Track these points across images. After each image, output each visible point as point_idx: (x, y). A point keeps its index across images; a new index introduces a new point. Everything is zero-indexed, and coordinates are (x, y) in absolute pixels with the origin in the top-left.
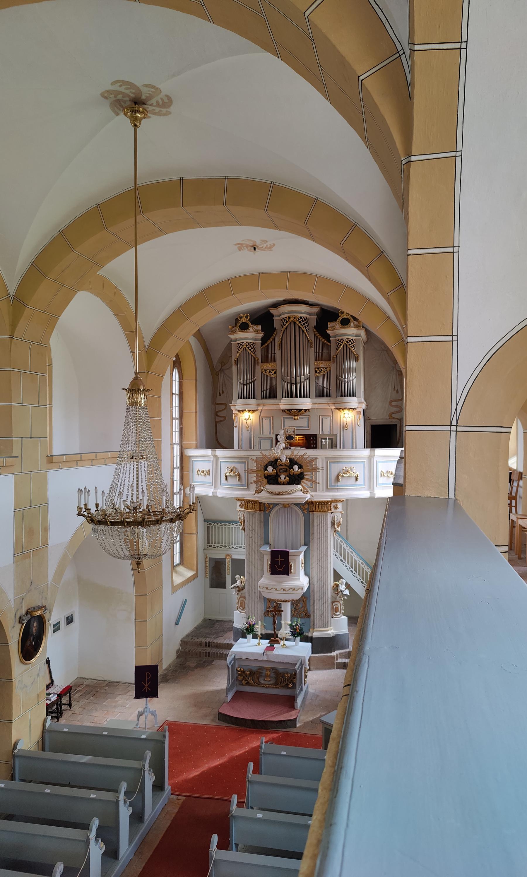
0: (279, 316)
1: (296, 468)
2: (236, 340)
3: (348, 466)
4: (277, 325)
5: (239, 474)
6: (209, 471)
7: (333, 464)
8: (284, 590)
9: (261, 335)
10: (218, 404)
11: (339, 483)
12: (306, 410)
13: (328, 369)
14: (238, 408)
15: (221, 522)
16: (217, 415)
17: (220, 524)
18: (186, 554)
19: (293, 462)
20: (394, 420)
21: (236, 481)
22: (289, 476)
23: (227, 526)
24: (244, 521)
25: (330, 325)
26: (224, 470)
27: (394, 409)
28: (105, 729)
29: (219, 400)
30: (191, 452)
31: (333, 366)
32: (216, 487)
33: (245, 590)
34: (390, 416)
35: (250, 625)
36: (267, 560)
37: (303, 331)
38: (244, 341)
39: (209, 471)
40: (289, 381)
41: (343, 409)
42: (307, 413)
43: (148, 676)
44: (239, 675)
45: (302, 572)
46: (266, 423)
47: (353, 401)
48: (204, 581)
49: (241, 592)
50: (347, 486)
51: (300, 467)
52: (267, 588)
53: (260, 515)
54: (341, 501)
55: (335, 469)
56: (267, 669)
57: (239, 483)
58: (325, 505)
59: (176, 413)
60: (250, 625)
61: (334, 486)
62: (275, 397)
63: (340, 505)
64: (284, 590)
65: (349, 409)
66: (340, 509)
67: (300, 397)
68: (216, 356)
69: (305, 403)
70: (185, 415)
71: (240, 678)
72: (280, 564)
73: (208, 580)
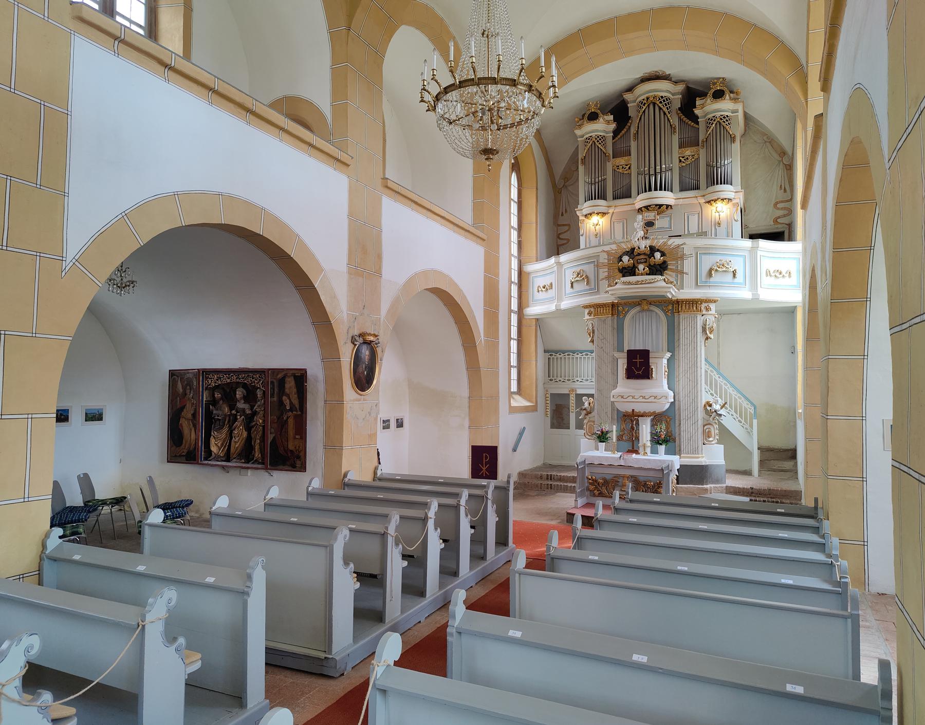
0: (635, 101)
1: (658, 255)
2: (582, 136)
3: (725, 259)
4: (631, 113)
5: (587, 277)
6: (551, 284)
7: (703, 256)
8: (644, 397)
9: (613, 126)
10: (559, 225)
11: (712, 279)
12: (668, 206)
13: (696, 157)
14: (585, 212)
16: (558, 237)
18: (525, 383)
19: (653, 249)
20: (780, 226)
21: (582, 286)
22: (650, 266)
24: (593, 332)
25: (698, 102)
26: (569, 276)
27: (781, 213)
28: (441, 478)
29: (562, 220)
30: (530, 268)
31: (702, 153)
32: (560, 299)
33: (594, 414)
34: (775, 221)
35: (602, 432)
36: (622, 364)
37: (665, 114)
38: (593, 134)
39: (551, 284)
40: (647, 172)
41: (715, 201)
42: (669, 211)
43: (486, 458)
44: (590, 484)
45: (665, 382)
46: (618, 227)
47: (727, 190)
48: (542, 418)
50: (721, 283)
51: (663, 254)
53: (613, 320)
54: (715, 301)
55: (707, 262)
56: (624, 477)
57: (588, 287)
58: (694, 304)
59: (514, 222)
60: (602, 432)
61: (706, 282)
62: (628, 195)
63: (713, 306)
64: (644, 397)
65: (723, 200)
66: (713, 312)
67: (661, 189)
68: (559, 170)
69: (666, 197)
70: (524, 227)
71: (592, 487)
72: (639, 366)
73: (548, 420)
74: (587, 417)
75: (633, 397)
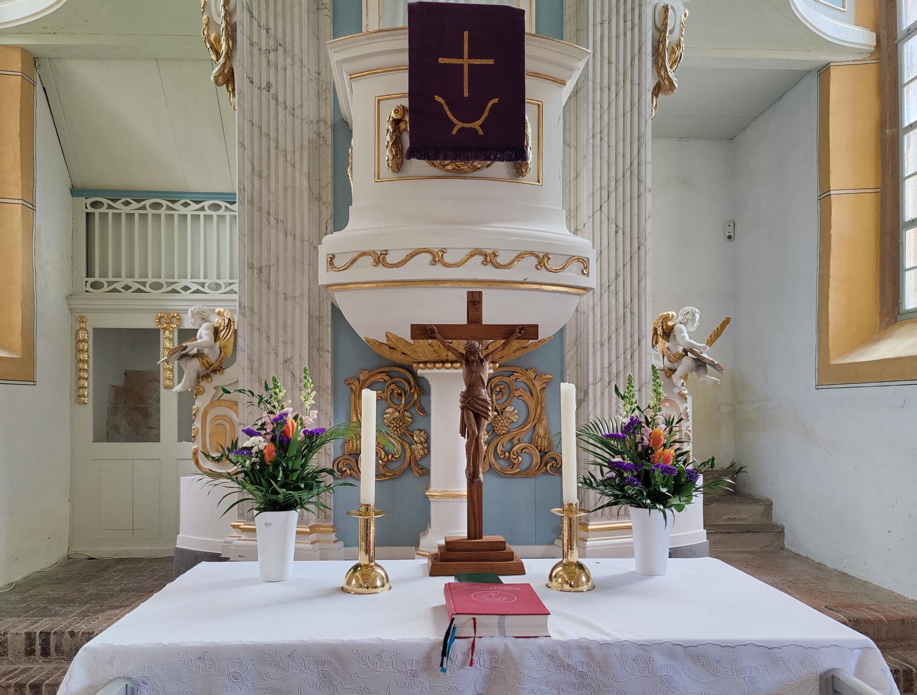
8: (490, 259)
15: (139, 196)
17: (135, 205)
23: (163, 212)
35: (281, 441)
49: (218, 380)
52: (380, 259)
60: (281, 441)
64: (490, 259)
74: (210, 388)
75: (437, 258)
